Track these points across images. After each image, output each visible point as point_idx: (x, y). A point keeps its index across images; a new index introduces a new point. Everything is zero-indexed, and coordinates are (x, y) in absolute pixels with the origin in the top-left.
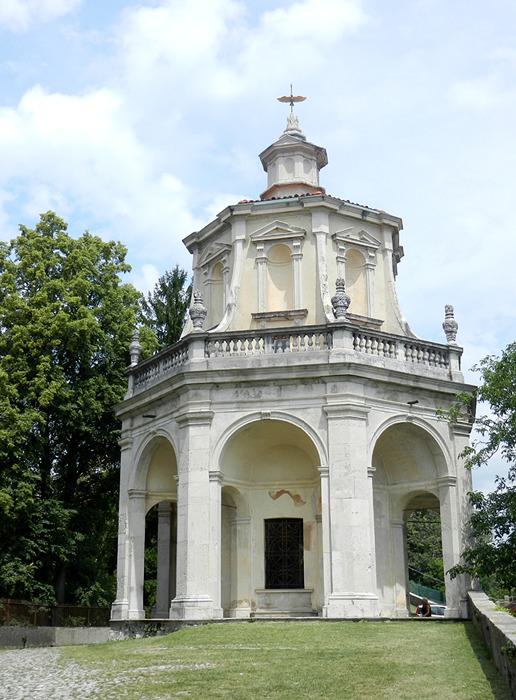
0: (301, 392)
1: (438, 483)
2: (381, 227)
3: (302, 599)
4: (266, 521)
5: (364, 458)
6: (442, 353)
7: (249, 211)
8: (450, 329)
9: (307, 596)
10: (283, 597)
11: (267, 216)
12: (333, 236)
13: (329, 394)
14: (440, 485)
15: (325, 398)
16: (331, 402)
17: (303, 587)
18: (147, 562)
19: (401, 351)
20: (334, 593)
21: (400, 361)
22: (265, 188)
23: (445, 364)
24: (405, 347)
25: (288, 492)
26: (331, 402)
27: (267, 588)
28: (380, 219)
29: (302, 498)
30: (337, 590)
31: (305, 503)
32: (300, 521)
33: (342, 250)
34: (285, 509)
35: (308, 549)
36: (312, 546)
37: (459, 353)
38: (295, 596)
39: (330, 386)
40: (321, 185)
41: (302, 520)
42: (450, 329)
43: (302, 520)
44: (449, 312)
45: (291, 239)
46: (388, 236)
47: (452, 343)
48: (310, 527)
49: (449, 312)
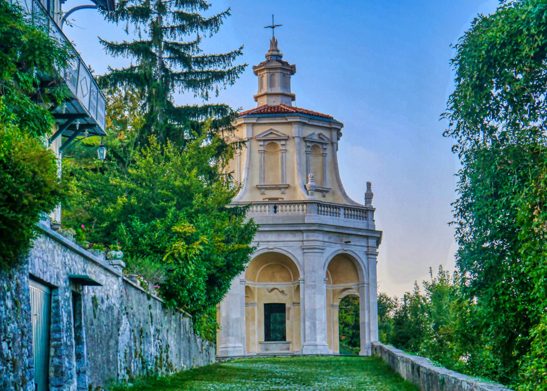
0: (289, 237)
1: (358, 285)
2: (330, 129)
3: (285, 346)
4: (265, 305)
5: (322, 273)
6: (364, 211)
7: (255, 121)
8: (369, 197)
9: (287, 345)
10: (274, 345)
11: (265, 124)
12: (304, 138)
13: (305, 239)
14: (360, 286)
15: (303, 241)
16: (306, 243)
17: (285, 340)
18: (343, 324)
19: (342, 211)
20: (306, 342)
21: (341, 220)
22: (256, 93)
23: (366, 217)
24: (345, 209)
25: (277, 289)
26: (306, 243)
27: (265, 340)
28: (330, 125)
29: (286, 292)
30: (308, 340)
31: (287, 295)
32: (284, 305)
33: (309, 146)
34: (275, 298)
35: (288, 319)
36: (291, 318)
37: (373, 211)
38: (281, 345)
39: (305, 235)
40: (292, 92)
41: (284, 304)
42: (369, 197)
43: (284, 304)
44: (369, 185)
45: (280, 140)
46: (335, 133)
47: (368, 206)
48: (289, 309)
49: (369, 185)
